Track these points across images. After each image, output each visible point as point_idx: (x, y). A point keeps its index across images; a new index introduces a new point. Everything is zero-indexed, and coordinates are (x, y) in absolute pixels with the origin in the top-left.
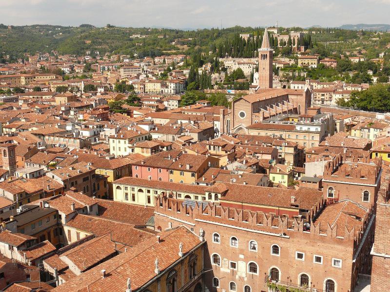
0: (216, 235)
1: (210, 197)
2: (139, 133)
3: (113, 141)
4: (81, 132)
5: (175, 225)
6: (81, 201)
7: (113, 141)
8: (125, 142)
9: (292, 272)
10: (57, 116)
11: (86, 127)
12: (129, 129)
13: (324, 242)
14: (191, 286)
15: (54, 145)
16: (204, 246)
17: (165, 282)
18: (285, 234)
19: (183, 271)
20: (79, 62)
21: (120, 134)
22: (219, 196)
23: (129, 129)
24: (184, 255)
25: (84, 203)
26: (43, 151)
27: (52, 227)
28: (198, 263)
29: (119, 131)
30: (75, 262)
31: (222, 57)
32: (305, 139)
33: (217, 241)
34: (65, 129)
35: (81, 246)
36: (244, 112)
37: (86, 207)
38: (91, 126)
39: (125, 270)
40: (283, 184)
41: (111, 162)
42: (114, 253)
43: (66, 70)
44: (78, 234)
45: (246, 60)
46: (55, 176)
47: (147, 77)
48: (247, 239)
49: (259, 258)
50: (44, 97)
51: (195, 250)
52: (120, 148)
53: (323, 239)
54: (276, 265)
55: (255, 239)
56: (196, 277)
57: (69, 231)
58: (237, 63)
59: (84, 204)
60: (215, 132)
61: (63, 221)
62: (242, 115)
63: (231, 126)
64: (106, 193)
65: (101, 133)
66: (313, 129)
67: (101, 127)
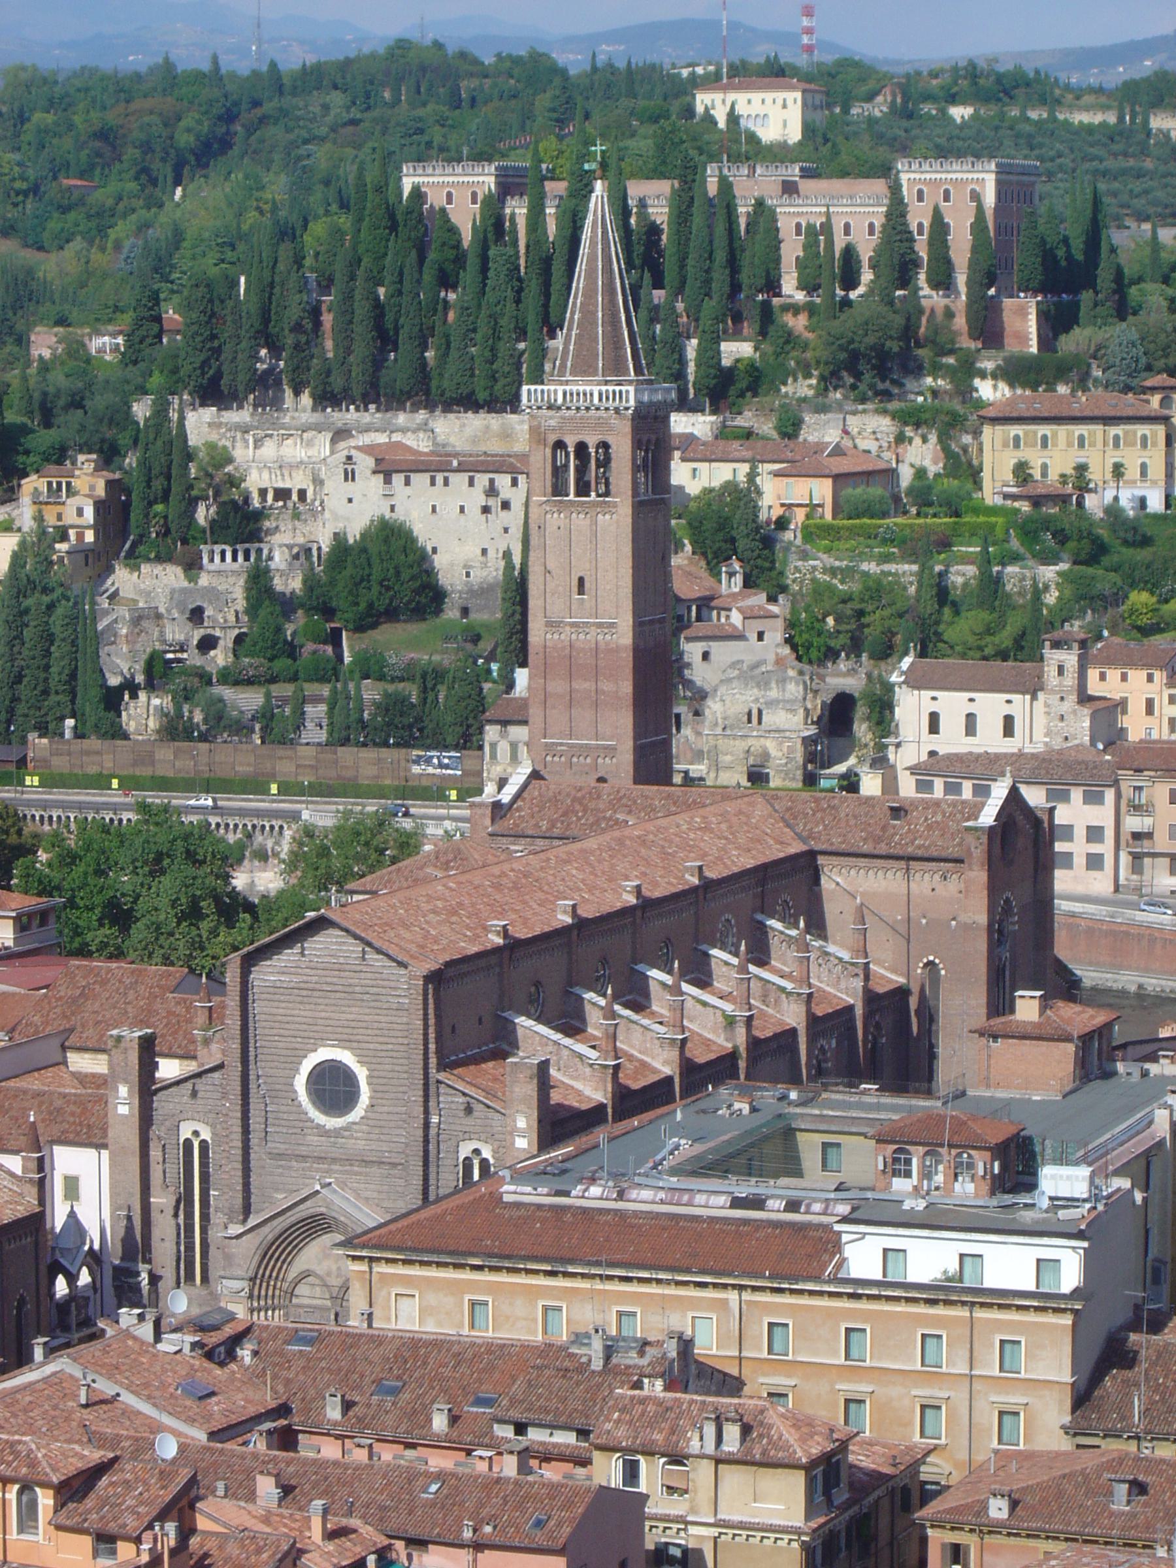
31: (213, 393)
32: (930, 1374)
36: (346, 1057)
45: (459, 430)
58: (364, 463)
60: (56, 1268)
62: (333, 1087)
63: (225, 1196)
66: (1008, 1264)
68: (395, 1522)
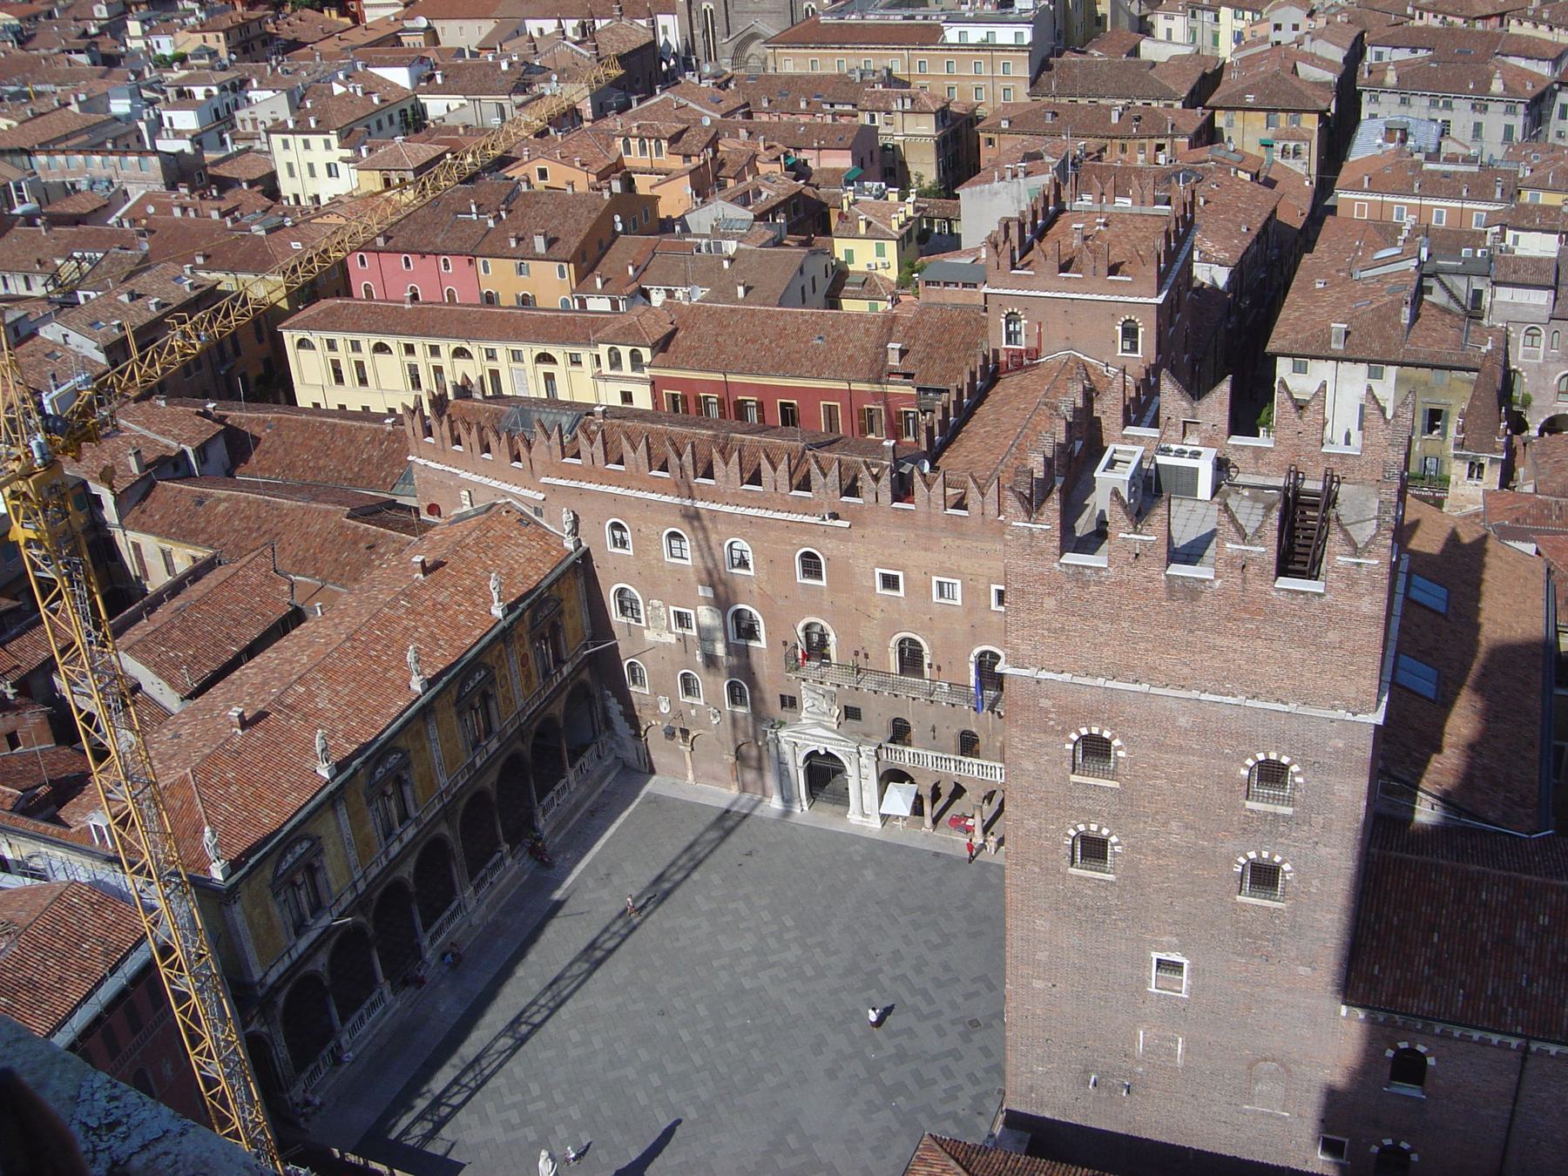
0: (616, 526)
1: (616, 362)
2: (376, 100)
3: (286, 145)
4: (165, 115)
5: (482, 501)
6: (163, 433)
7: (286, 145)
9: (869, 634)
10: (79, 52)
11: (181, 94)
12: (338, 89)
13: (961, 536)
14: (550, 700)
15: (73, 185)
16: (582, 568)
17: (453, 711)
18: (835, 516)
19: (515, 660)
21: (309, 113)
22: (646, 354)
23: (338, 89)
24: (511, 608)
25: (175, 438)
26: (29, 219)
28: (569, 624)
29: (302, 99)
30: (159, 669)
32: (978, 77)
33: (623, 543)
34: (109, 110)
35: (177, 602)
37: (184, 452)
38: (199, 93)
39: (311, 696)
40: (881, 272)
41: (272, 243)
42: (289, 614)
44: (166, 555)
49: (763, 595)
51: (550, 586)
52: (311, 166)
53: (956, 527)
54: (820, 614)
55: (743, 536)
56: (566, 670)
57: (137, 547)
59: (174, 444)
60: (662, 60)
61: (110, 513)
63: (720, 28)
65: (239, 115)
66: (1005, 35)
67: (240, 86)
68: (790, 142)
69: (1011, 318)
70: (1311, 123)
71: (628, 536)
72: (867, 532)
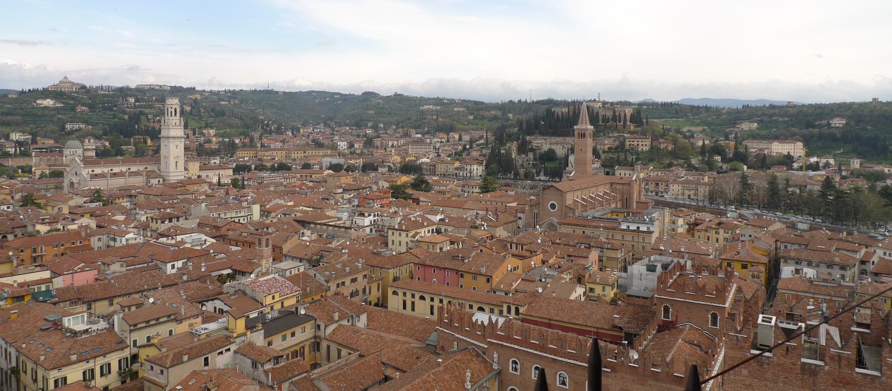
0: (515, 363)
1: (509, 311)
5: (462, 346)
8: (407, 236)
13: (657, 380)
20: (358, 136)
22: (521, 310)
27: (307, 340)
31: (529, 134)
33: (516, 370)
43: (343, 145)
44: (339, 351)
46: (317, 275)
47: (439, 156)
48: (554, 371)
50: (313, 176)
57: (328, 347)
62: (553, 206)
64: (378, 299)
69: (666, 310)
70: (763, 268)
71: (518, 367)
72: (617, 375)
